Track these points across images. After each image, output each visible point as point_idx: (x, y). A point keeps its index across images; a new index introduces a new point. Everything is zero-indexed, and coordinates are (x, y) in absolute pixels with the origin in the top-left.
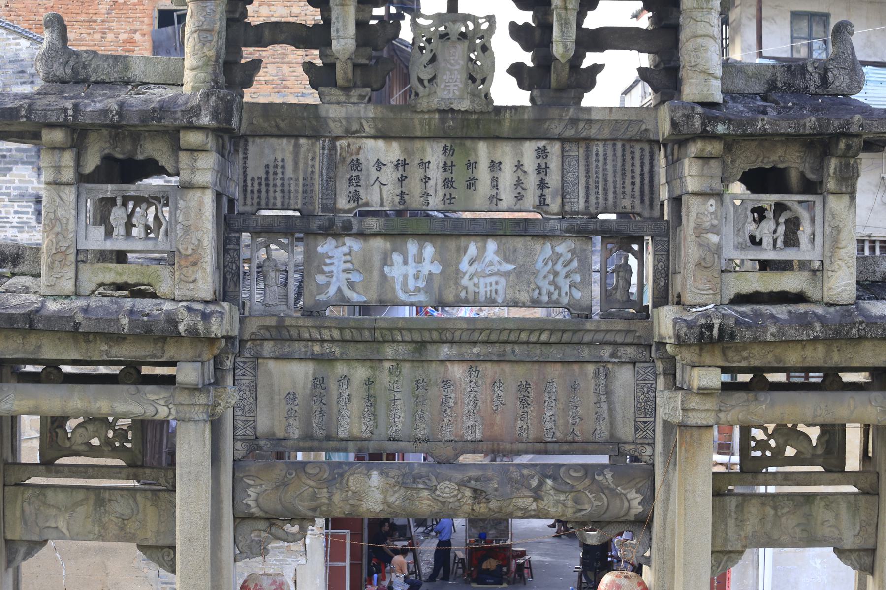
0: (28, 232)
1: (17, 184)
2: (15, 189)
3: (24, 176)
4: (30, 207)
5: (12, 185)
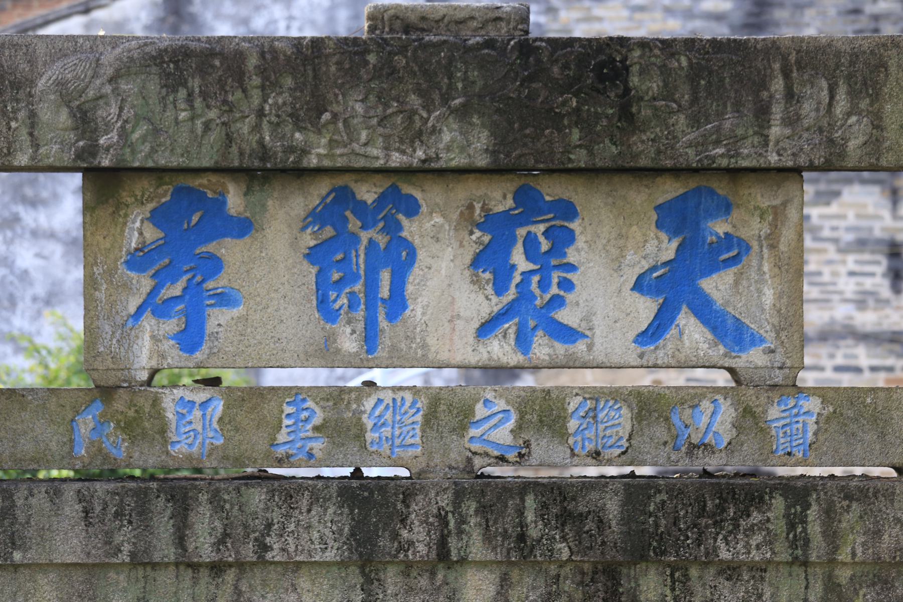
0: (875, 309)
1: (851, 220)
2: (849, 229)
3: (865, 206)
4: (878, 263)
5: (842, 224)
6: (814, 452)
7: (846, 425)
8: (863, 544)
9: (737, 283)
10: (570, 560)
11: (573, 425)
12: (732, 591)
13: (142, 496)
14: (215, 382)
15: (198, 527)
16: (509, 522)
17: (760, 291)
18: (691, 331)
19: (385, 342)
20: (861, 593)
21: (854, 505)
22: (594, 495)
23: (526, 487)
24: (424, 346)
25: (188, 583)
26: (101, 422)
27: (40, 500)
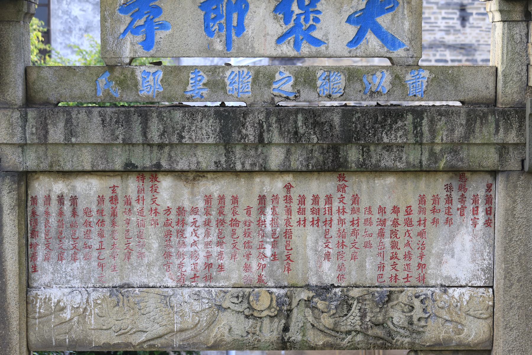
0: (454, 34)
4: (455, 13)
6: (426, 95)
7: (440, 83)
8: (447, 135)
9: (393, 19)
10: (317, 143)
11: (319, 83)
12: (389, 156)
13: (127, 114)
14: (159, 64)
15: (152, 128)
16: (290, 126)
17: (403, 23)
18: (372, 41)
19: (235, 45)
20: (445, 156)
21: (443, 118)
22: (328, 114)
23: (297, 111)
24: (253, 47)
25: (148, 152)
26: (109, 80)
27: (83, 115)
